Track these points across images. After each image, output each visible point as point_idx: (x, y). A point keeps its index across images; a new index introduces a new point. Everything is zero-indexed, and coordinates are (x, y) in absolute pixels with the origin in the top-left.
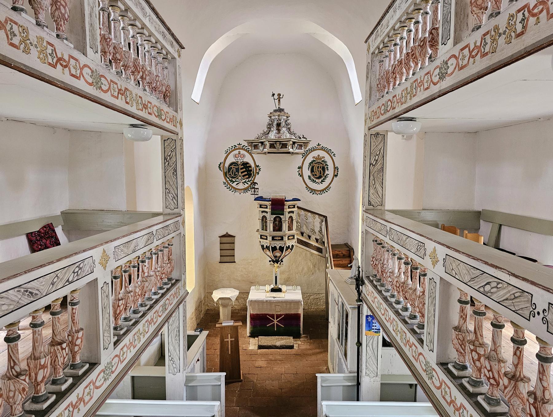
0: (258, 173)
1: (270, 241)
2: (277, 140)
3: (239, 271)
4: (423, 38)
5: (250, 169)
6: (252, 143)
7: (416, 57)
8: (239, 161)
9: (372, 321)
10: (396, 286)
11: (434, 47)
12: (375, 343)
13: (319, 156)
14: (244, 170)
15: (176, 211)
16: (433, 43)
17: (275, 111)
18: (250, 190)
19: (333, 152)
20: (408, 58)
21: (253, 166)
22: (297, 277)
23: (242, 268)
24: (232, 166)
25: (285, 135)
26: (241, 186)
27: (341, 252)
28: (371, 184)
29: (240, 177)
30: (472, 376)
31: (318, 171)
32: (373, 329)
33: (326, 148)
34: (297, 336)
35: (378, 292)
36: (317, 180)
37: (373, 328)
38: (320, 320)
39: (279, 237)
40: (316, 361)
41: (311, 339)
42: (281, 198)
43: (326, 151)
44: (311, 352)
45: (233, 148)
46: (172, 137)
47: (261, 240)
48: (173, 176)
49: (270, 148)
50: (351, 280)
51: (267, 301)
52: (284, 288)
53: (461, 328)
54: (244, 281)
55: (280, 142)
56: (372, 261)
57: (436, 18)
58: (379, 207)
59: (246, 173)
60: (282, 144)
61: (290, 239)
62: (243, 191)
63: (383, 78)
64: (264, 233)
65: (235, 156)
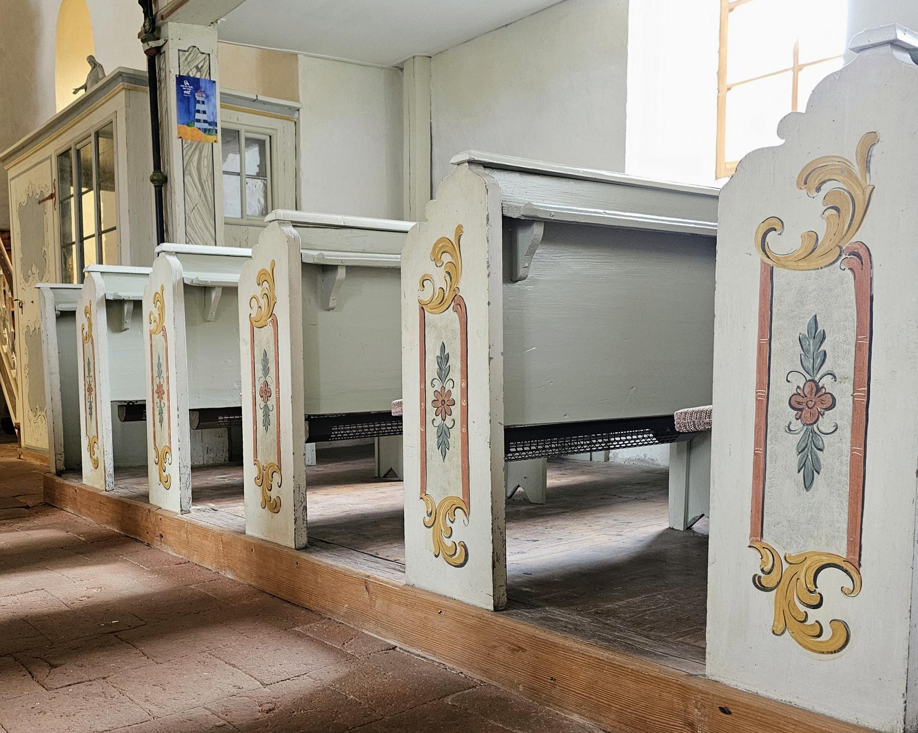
9: (193, 94)
12: (206, 164)
32: (198, 121)
37: (198, 116)
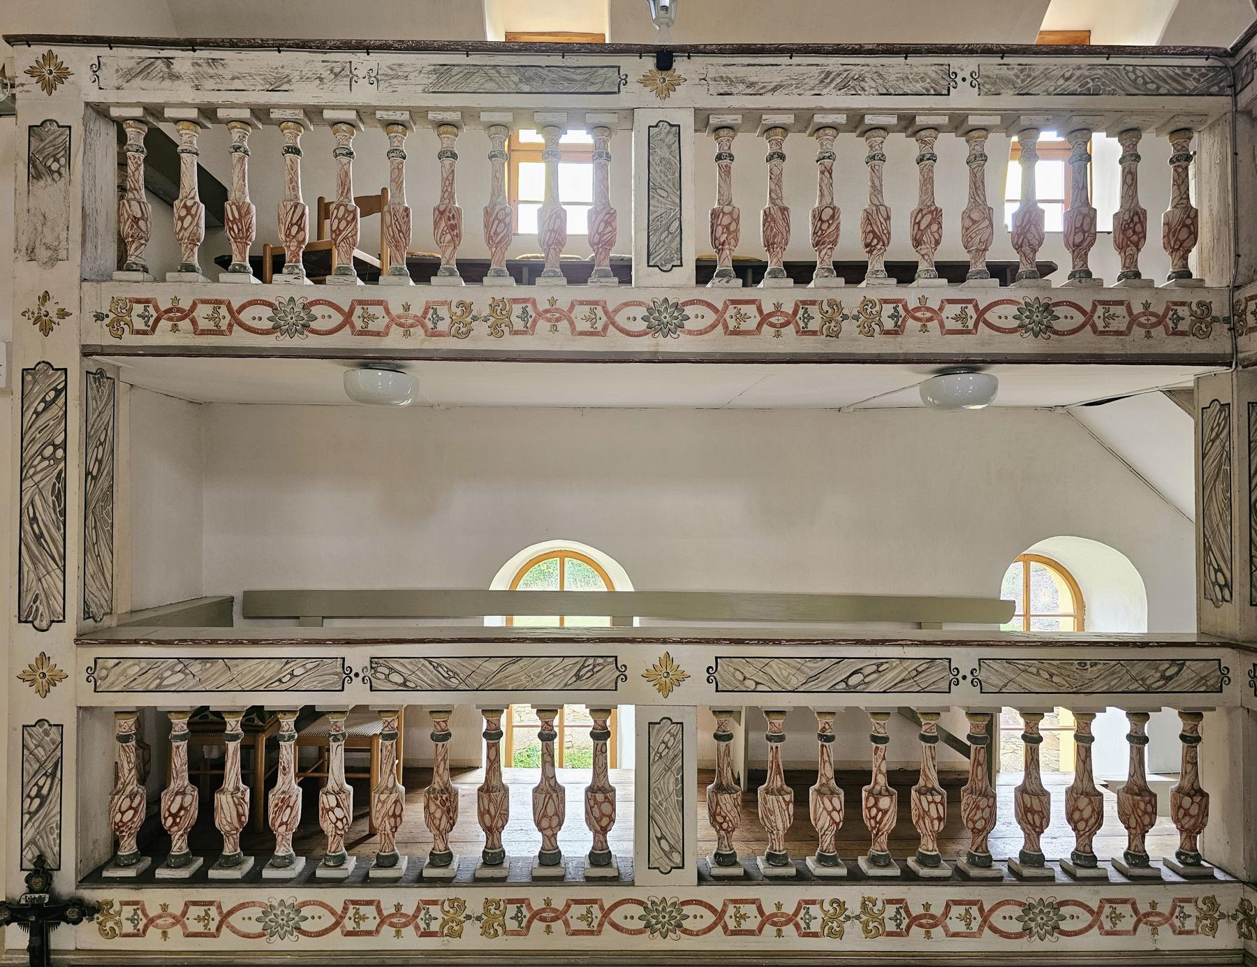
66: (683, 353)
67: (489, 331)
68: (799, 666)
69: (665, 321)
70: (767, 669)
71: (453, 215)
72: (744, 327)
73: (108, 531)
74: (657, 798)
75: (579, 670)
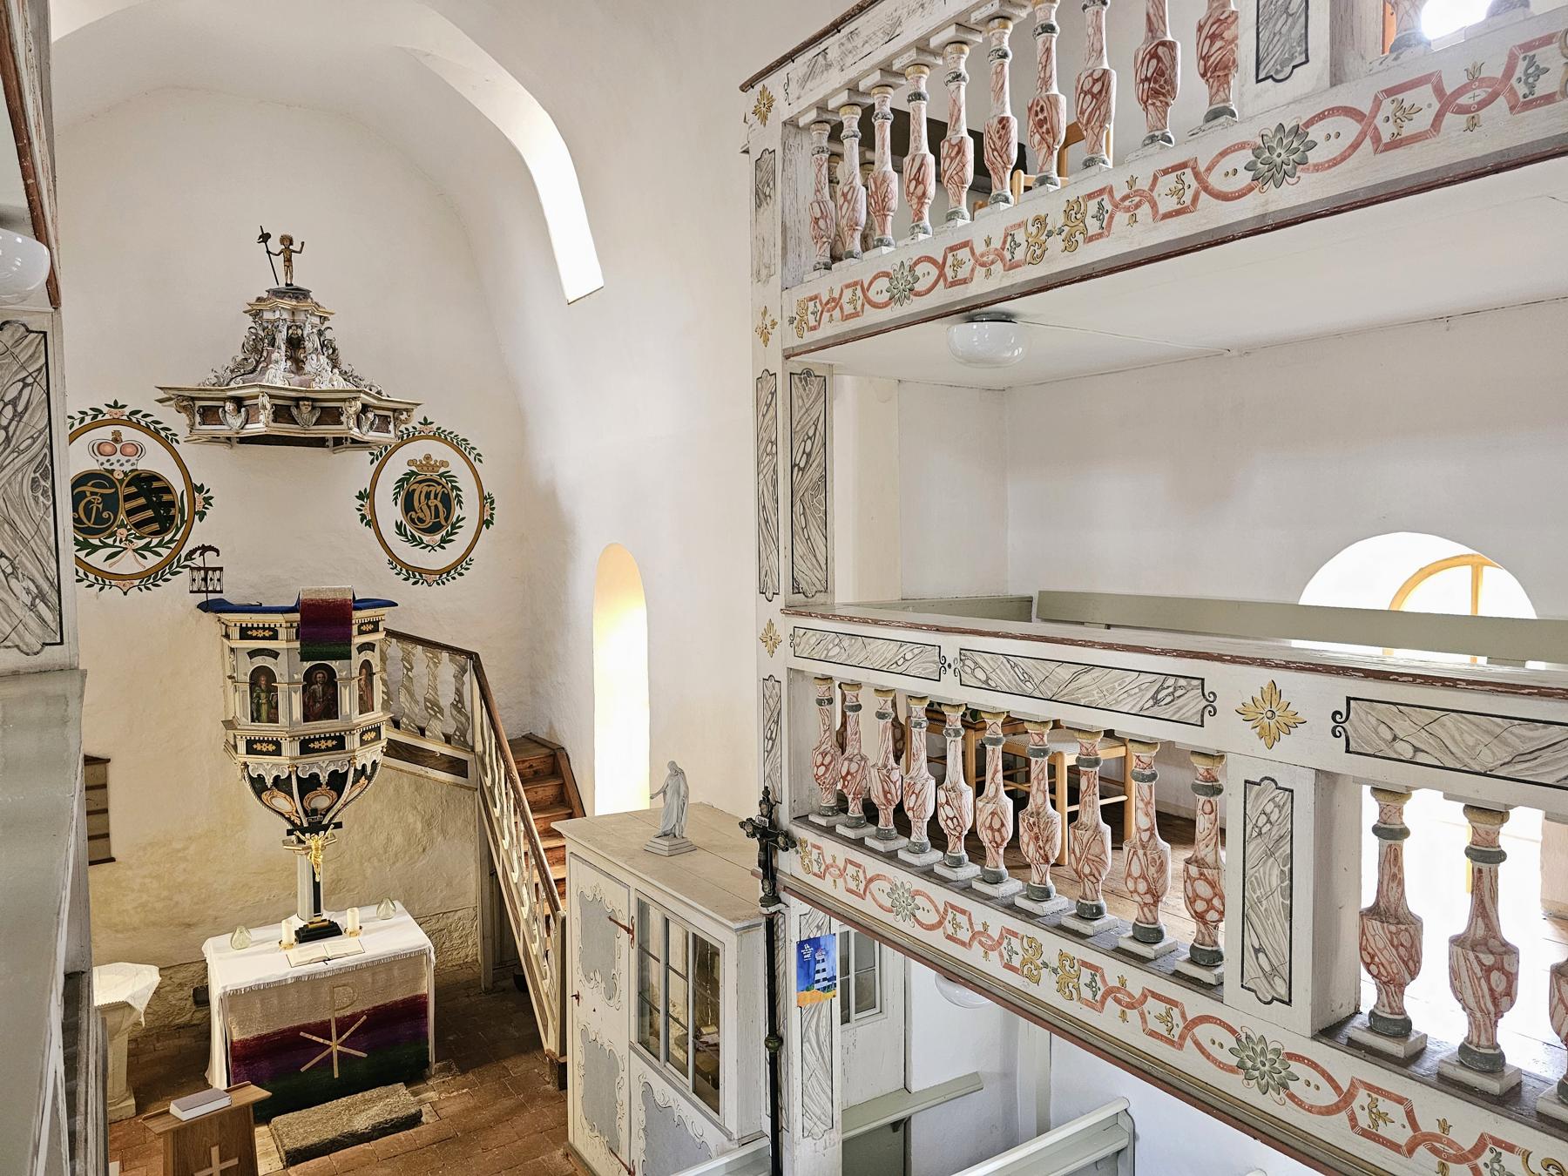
0: (202, 515)
1: (296, 758)
2: (303, 395)
3: (133, 890)
4: (1101, 73)
5: (166, 498)
6: (193, 399)
7: (1052, 128)
8: (116, 466)
9: (813, 956)
10: (991, 828)
11: (1162, 98)
13: (428, 457)
14: (142, 501)
15: (52, 655)
16: (1160, 86)
17: (277, 293)
18: (168, 576)
19: (474, 449)
20: (1002, 132)
21: (179, 486)
22: (369, 871)
23: (145, 877)
24: (87, 489)
25: (324, 380)
26: (128, 564)
27: (527, 764)
28: (797, 528)
29: (123, 530)
30: (1471, 1043)
31: (429, 507)
32: (818, 981)
33: (451, 433)
34: (414, 1075)
35: (884, 857)
36: (426, 539)
37: (818, 977)
38: (467, 1000)
39: (326, 739)
40: (519, 1143)
41: (464, 1071)
42: (339, 597)
43: (451, 445)
44: (486, 1114)
45: (88, 420)
46: (24, 319)
47: (252, 760)
48: (36, 499)
49: (275, 421)
50: (667, 843)
51: (298, 980)
52: (348, 919)
53: (1396, 910)
54: (154, 924)
55: (314, 400)
56: (822, 764)
57: (1161, 14)
58: (820, 598)
59: (150, 513)
60: (322, 408)
61: (368, 742)
62: (137, 582)
63: (849, 197)
64: (265, 730)
65: (98, 449)
66: (1304, 205)
67: (1062, 245)
68: (1498, 731)
69: (1279, 160)
70: (1435, 728)
71: (1042, 107)
72: (1409, 129)
73: (820, 517)
74: (1254, 892)
75: (1157, 692)
